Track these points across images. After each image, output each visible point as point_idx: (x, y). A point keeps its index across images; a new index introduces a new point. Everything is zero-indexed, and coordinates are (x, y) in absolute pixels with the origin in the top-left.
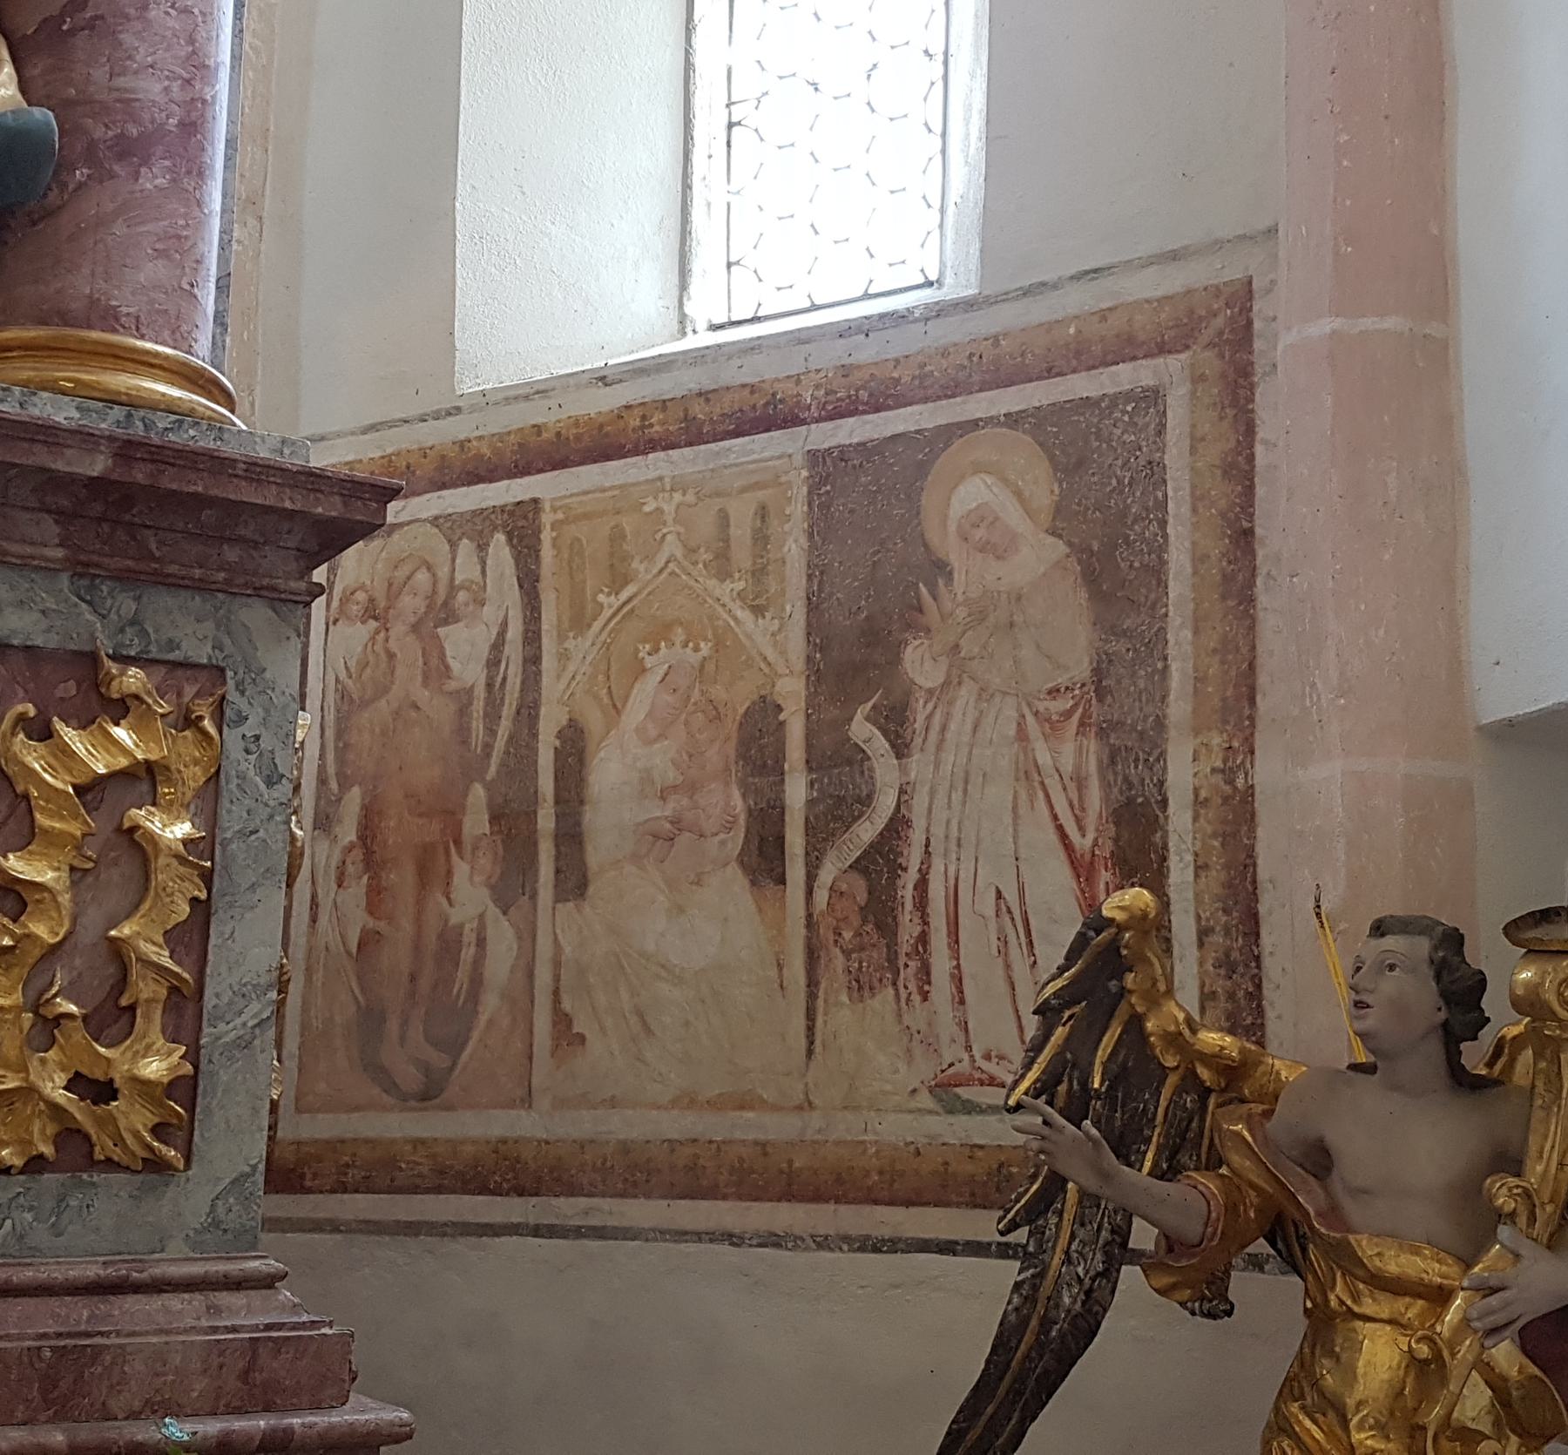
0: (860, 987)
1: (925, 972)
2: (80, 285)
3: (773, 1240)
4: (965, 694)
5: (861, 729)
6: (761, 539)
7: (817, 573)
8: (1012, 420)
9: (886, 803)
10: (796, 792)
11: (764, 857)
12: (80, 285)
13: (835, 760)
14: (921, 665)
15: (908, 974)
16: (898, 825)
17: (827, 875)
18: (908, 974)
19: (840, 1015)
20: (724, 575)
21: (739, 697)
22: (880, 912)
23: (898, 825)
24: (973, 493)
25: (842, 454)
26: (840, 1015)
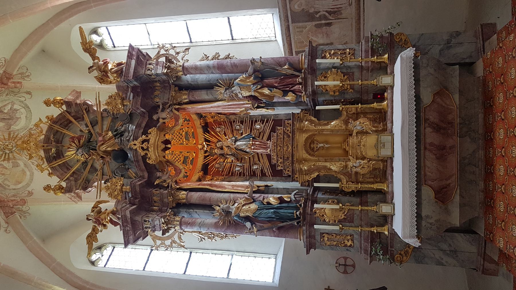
0: (341, 14)
1: (340, 8)
2: (297, 62)
3: (364, 20)
4: (315, 6)
5: (318, 16)
6: (300, 28)
7: (303, 22)
8: (290, 4)
9: (324, 13)
10: (323, 22)
11: (329, 25)
12: (297, 62)
13: (320, 19)
14: (312, 11)
15: (340, 9)
16: (326, 11)
17: (331, 18)
18: (340, 9)
19: (344, 16)
20: (303, 31)
21: (315, 28)
22: (334, 12)
23: (326, 11)
24: (296, 7)
25: (292, 20)
26: (344, 16)
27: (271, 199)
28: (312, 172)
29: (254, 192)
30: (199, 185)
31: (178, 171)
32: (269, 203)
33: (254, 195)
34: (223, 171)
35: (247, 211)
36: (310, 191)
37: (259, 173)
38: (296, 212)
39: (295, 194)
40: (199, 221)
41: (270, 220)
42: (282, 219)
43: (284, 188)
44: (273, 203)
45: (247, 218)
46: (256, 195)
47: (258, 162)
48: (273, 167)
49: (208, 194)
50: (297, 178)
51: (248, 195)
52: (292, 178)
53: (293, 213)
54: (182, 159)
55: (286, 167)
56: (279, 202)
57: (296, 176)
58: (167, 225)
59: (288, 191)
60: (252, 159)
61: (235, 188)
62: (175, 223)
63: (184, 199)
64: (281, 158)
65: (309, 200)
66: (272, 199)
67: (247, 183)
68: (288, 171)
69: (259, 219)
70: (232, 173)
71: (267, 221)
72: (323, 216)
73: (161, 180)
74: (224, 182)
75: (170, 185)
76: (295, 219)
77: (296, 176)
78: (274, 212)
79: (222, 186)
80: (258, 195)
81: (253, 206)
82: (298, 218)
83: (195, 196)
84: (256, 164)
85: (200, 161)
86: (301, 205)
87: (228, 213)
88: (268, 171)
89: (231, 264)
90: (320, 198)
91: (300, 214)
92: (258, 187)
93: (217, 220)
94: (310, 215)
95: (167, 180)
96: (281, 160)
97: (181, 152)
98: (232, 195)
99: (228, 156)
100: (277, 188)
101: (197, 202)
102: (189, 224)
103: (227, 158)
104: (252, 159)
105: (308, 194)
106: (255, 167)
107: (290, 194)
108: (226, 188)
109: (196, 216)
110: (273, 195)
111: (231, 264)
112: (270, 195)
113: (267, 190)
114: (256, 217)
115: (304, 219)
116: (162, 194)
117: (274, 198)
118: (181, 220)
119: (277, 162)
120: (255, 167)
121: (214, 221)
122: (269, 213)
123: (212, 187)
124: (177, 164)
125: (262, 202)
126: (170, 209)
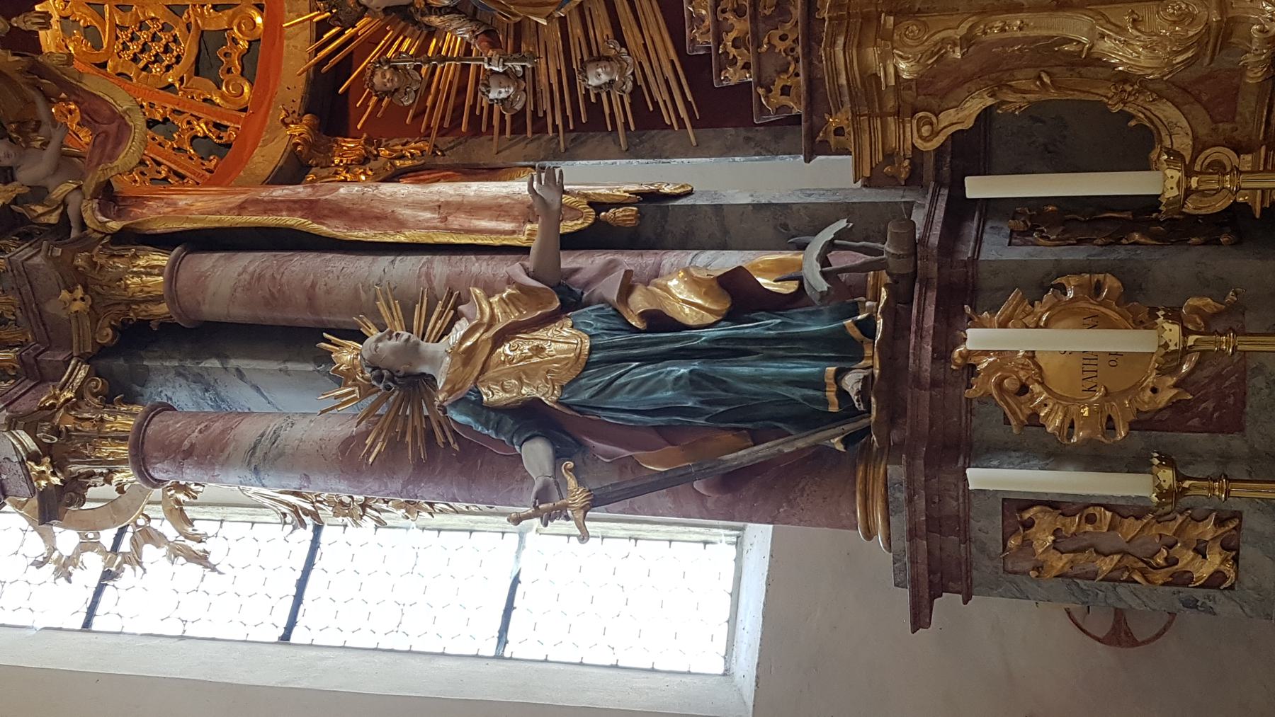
27: (673, 283)
28: (944, 94)
29: (572, 242)
30: (241, 208)
31: (108, 127)
32: (658, 321)
33: (569, 261)
34: (419, 115)
35: (524, 374)
36: (927, 216)
37: (619, 109)
38: (840, 374)
39: (830, 246)
40: (248, 431)
41: (668, 426)
42: (751, 417)
43: (758, 207)
44: (687, 315)
45: (529, 417)
46: (586, 263)
47: (613, 48)
48: (697, 68)
49: (301, 265)
50: (839, 131)
51: (530, 262)
52: (812, 134)
53: (819, 385)
54: (188, 48)
55: (769, 70)
56: (723, 306)
57: (833, 122)
58: (58, 466)
59: (784, 225)
60: (576, 31)
61: (458, 221)
62: (106, 451)
63: (157, 300)
64: (739, 12)
65: (926, 284)
66: (680, 286)
67: (518, 187)
68: (785, 91)
69: (606, 417)
70: (475, 120)
71: (657, 428)
72: (1024, 389)
73: (13, 189)
74: (387, 189)
75: (71, 212)
76: (835, 419)
77: (833, 122)
78: (695, 381)
79: (378, 208)
80: (599, 259)
81: (564, 341)
82: (848, 411)
83: (224, 279)
84: (601, 59)
85: (296, 59)
86: (867, 327)
87: (414, 385)
88: (672, 98)
89: (516, 581)
90: (999, 267)
91: (863, 394)
92: (598, 205)
93: (351, 428)
94: (934, 384)
95: (50, 183)
96: (740, 26)
97: (177, 10)
98: (441, 267)
99: (435, 20)
100: (718, 208)
101: (239, 313)
102: (189, 453)
103: (432, 32)
104: (576, 31)
105: (914, 248)
106: (597, 77)
107: (802, 247)
108: (401, 225)
109: (242, 396)
110: (685, 257)
111: (516, 581)
112: (670, 259)
113: (656, 223)
114: (582, 408)
115: (894, 413)
116: (26, 273)
117: (694, 283)
118: (141, 428)
119: (719, 40)
120: (597, 77)
121: (340, 427)
122: (661, 385)
123: (318, 218)
124: (94, 84)
125: (618, 315)
126: (86, 359)
